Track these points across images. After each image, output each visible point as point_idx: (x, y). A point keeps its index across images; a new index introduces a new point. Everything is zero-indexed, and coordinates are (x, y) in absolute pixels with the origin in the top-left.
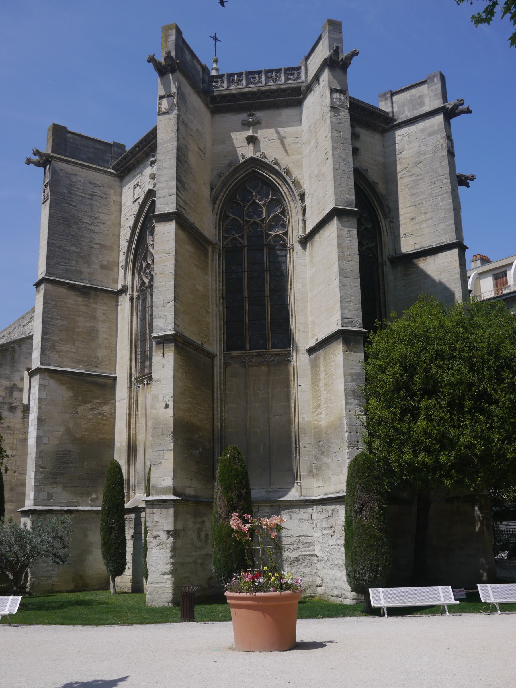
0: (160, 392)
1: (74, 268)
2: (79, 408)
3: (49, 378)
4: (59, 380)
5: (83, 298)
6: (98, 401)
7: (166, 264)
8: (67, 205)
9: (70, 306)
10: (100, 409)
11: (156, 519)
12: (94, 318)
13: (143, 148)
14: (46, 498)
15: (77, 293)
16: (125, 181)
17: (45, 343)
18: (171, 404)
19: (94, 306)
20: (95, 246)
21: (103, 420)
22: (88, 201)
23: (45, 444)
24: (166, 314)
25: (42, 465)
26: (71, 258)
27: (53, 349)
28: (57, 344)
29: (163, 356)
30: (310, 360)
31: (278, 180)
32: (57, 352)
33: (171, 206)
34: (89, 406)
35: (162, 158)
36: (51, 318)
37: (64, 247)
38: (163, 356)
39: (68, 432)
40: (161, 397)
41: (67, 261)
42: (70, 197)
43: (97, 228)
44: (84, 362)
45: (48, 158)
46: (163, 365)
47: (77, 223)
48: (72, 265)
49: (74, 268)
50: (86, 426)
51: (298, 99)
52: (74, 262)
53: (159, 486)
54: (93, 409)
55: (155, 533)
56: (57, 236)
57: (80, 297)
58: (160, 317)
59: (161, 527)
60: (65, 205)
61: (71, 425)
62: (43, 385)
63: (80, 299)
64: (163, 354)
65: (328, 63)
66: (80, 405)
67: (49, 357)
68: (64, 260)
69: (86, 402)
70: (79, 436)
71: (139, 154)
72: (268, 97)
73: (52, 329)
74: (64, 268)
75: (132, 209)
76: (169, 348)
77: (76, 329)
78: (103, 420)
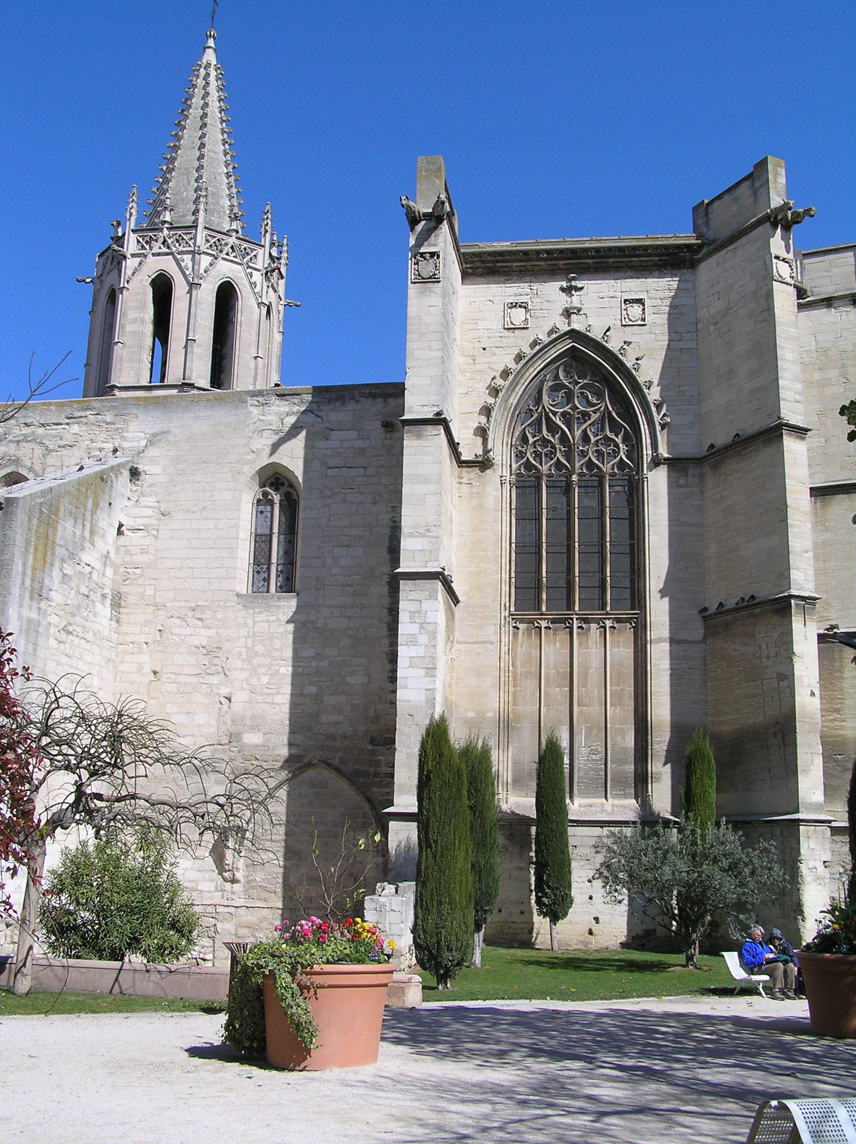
11: (812, 846)
16: (467, 281)
18: (817, 692)
30: (819, 648)
40: (805, 679)
53: (809, 801)
58: (797, 569)
71: (542, 263)
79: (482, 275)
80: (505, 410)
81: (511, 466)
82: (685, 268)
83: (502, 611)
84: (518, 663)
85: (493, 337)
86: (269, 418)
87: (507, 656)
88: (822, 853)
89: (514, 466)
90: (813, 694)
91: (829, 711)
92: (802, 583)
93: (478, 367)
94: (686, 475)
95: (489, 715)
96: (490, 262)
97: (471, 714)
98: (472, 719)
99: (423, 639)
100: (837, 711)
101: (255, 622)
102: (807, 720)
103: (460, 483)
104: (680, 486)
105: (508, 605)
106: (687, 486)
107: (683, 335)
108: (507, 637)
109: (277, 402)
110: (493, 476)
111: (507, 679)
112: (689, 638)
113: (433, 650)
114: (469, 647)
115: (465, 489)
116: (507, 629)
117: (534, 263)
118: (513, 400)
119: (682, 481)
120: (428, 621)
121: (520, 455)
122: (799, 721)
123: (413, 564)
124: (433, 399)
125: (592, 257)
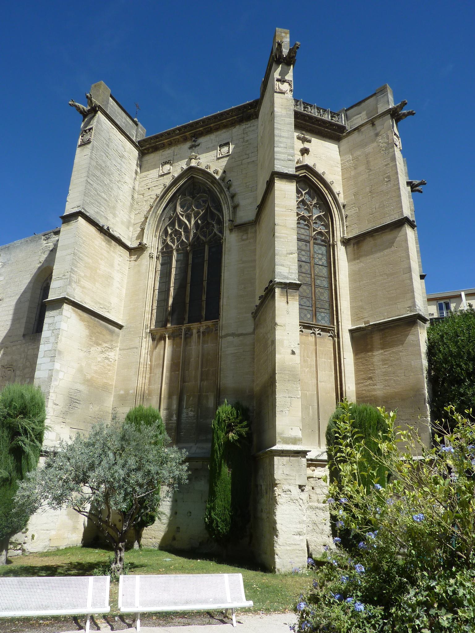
0: (285, 338)
1: (103, 213)
2: (93, 349)
3: (72, 311)
4: (80, 315)
5: (106, 243)
6: (106, 345)
7: (287, 219)
8: (104, 155)
9: (96, 247)
10: (107, 353)
12: (112, 266)
13: (185, 132)
14: (54, 439)
15: (103, 238)
17: (72, 275)
19: (113, 254)
20: (119, 201)
21: (109, 365)
22: (119, 161)
23: (61, 379)
24: (289, 263)
25: (55, 402)
26: (102, 203)
27: (78, 283)
28: (82, 280)
29: (288, 303)
31: (325, 189)
32: (81, 287)
33: (290, 169)
34: (99, 349)
35: (280, 128)
36: (81, 253)
37: (98, 192)
38: (288, 303)
39: (80, 370)
40: (286, 343)
41: (99, 205)
42: (107, 150)
43: (122, 186)
44: (100, 304)
45: (96, 107)
46: (288, 313)
47: (109, 175)
48: (102, 210)
49: (103, 213)
50: (95, 368)
51: (340, 136)
52: (103, 208)
54: (102, 352)
55: (286, 487)
56: (95, 178)
57: (105, 242)
58: (283, 265)
59: (292, 481)
60: (103, 154)
61: (84, 364)
62: (66, 316)
63: (104, 243)
64: (287, 301)
65: (391, 112)
66: (92, 346)
67: (74, 290)
68: (97, 203)
69: (98, 344)
70: (89, 377)
71: (178, 137)
72: (320, 125)
73: (80, 263)
74: (96, 210)
75: (157, 181)
76: (294, 296)
77: (98, 271)
78: (109, 365)
79: (152, 152)
80: (155, 217)
81: (158, 248)
82: (253, 119)
83: (144, 329)
84: (153, 359)
85: (154, 181)
86: (49, 244)
87: (146, 355)
88: (297, 478)
89: (160, 248)
90: (293, 353)
91: (365, 379)
92: (286, 274)
93: (145, 199)
94: (247, 233)
95: (131, 392)
96: (153, 143)
97: (122, 392)
98: (122, 395)
99: (52, 340)
100: (370, 378)
101: (28, 350)
102: (287, 372)
103: (130, 261)
104: (243, 240)
105: (149, 325)
106: (247, 239)
107: (250, 155)
108: (147, 344)
109: (54, 236)
110: (146, 254)
111: (145, 369)
112: (244, 332)
113: (56, 345)
114: (125, 352)
115: (133, 263)
116: (148, 339)
117: (174, 138)
118: (160, 211)
119: (244, 237)
120: (56, 328)
121: (164, 242)
122: (279, 373)
123: (54, 295)
124: (78, 203)
125: (202, 126)
